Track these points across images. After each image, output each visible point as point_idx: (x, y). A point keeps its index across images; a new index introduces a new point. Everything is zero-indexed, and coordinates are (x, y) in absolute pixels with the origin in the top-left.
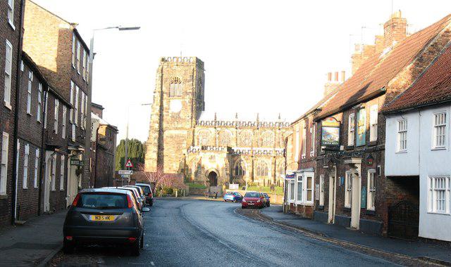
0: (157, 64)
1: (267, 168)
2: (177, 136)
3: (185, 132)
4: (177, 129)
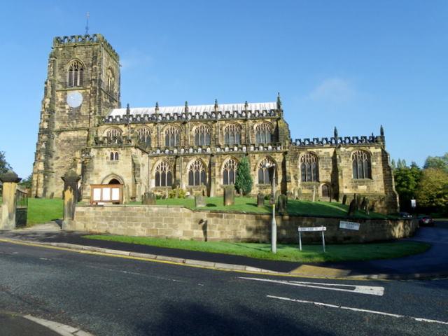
0: (48, 47)
4: (76, 129)
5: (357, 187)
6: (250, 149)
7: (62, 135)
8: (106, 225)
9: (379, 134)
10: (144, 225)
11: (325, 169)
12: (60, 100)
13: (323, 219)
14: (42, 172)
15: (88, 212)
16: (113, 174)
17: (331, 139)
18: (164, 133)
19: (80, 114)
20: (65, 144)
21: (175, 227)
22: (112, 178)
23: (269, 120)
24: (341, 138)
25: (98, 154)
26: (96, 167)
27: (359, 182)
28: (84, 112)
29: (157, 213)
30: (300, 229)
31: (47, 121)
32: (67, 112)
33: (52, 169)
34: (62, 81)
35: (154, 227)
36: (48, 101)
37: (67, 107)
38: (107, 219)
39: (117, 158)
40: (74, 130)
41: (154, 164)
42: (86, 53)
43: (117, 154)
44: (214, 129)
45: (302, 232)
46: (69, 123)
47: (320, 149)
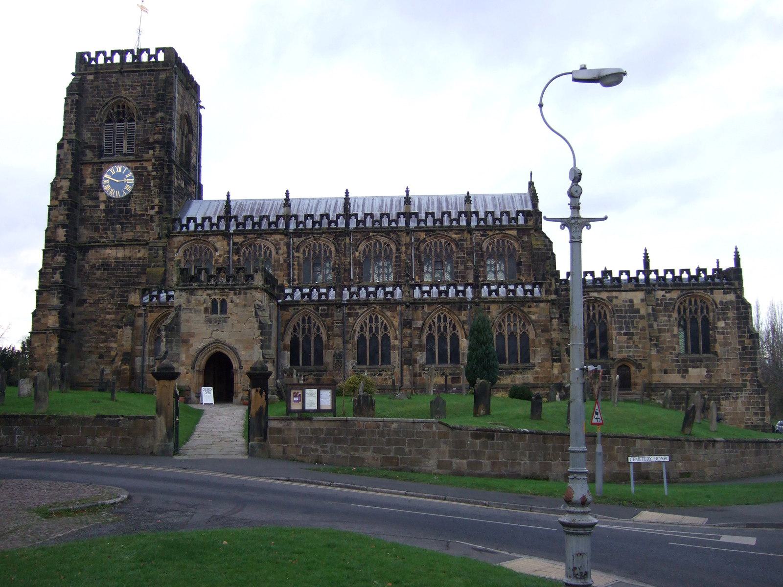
0: (66, 74)
1: (386, 338)
2: (122, 263)
3: (142, 253)
5: (686, 372)
6: (480, 293)
7: (92, 254)
8: (317, 450)
9: (732, 265)
10: (376, 451)
11: (626, 334)
12: (89, 181)
13: (648, 442)
14: (54, 331)
15: (289, 429)
16: (217, 341)
17: (638, 272)
18: (301, 256)
19: (128, 211)
20: (98, 273)
21: (425, 454)
23: (514, 233)
24: (656, 272)
25: (189, 301)
26: (184, 328)
27: (692, 361)
28: (135, 207)
29: (396, 432)
30: (631, 459)
31: (64, 226)
32: (102, 206)
33: (72, 324)
34: (94, 142)
35: (392, 455)
36: (65, 184)
37: (102, 197)
38: (318, 441)
39: (224, 310)
40: (116, 246)
41: (288, 321)
42: (143, 85)
43: (224, 302)
44: (403, 248)
45: (635, 464)
46: (105, 230)
47: (614, 294)
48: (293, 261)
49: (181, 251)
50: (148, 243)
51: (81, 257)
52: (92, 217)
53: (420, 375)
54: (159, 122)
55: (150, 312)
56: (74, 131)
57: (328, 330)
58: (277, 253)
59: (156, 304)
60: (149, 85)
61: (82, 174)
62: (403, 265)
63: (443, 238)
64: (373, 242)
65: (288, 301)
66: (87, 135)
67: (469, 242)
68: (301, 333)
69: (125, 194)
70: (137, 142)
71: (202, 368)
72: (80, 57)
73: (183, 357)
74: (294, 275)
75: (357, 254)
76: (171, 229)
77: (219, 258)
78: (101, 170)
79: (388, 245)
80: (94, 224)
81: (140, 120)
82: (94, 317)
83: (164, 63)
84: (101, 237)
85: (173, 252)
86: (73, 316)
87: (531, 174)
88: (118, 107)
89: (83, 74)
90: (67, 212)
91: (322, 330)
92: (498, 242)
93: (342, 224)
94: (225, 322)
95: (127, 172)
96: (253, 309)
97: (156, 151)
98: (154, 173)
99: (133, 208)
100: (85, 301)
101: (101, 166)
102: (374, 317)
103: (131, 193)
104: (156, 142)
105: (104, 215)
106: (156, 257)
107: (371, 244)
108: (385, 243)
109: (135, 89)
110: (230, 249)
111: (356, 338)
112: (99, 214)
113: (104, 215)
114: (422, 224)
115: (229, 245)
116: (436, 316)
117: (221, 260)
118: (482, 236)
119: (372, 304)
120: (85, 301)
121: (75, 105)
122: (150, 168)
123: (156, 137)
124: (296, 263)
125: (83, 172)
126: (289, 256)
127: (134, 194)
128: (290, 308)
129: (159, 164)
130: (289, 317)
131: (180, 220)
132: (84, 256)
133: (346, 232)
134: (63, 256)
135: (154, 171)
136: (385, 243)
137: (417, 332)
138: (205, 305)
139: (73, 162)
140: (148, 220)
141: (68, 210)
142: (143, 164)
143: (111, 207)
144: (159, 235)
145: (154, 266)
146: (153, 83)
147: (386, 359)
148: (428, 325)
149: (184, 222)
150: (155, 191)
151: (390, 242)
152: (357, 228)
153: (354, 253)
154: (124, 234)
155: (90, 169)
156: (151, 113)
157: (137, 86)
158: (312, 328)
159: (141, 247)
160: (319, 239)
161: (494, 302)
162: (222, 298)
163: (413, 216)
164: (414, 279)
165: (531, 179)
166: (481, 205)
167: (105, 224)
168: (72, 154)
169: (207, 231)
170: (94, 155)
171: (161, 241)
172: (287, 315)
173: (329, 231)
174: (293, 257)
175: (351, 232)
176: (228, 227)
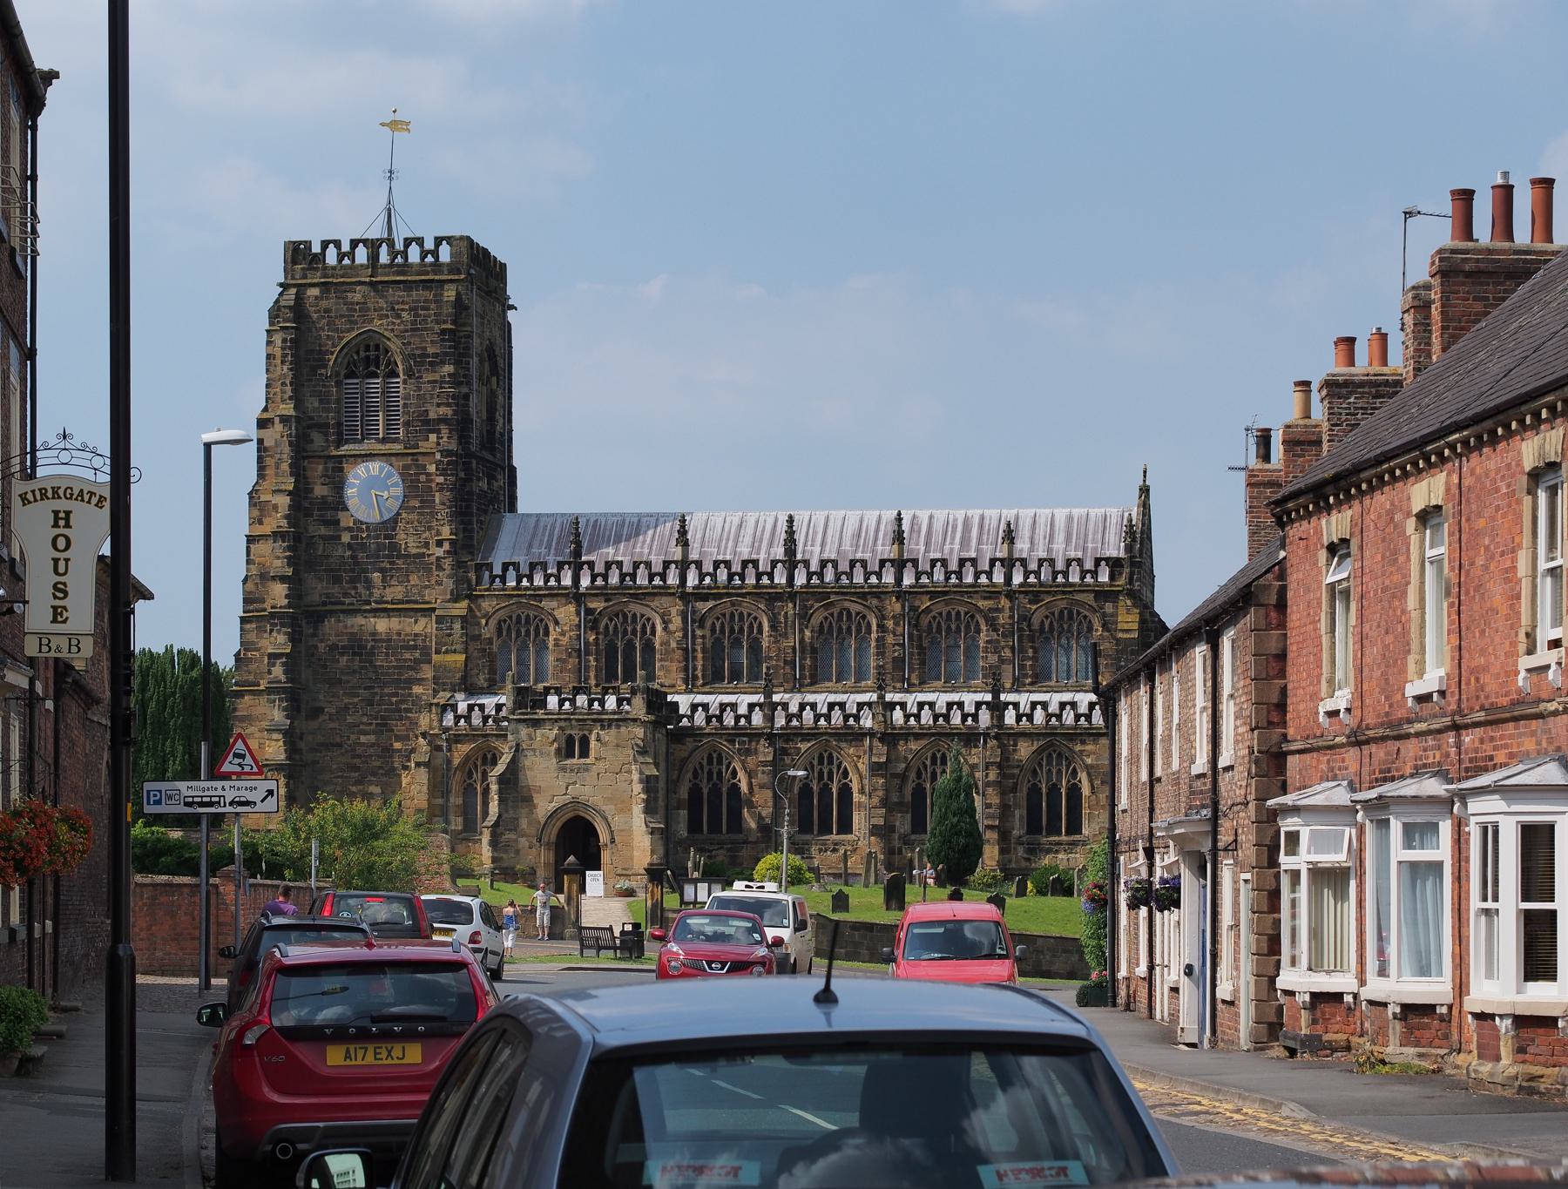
1: (845, 792)
6: (1002, 717)
7: (330, 625)
12: (320, 490)
16: (575, 802)
18: (708, 633)
19: (394, 547)
20: (344, 660)
22: (571, 815)
28: (408, 541)
31: (283, 579)
37: (346, 521)
39: (585, 753)
41: (684, 761)
43: (585, 742)
44: (890, 624)
46: (353, 581)
48: (694, 643)
49: (493, 622)
50: (434, 610)
51: (311, 631)
52: (327, 557)
53: (900, 852)
54: (446, 382)
55: (457, 742)
56: (290, 398)
57: (750, 777)
58: (665, 629)
59: (465, 729)
60: (423, 309)
61: (305, 478)
62: (889, 655)
63: (961, 605)
64: (836, 611)
65: (685, 728)
66: (313, 403)
67: (1007, 613)
68: (705, 781)
69: (387, 516)
70: (407, 417)
71: (553, 838)
72: (297, 253)
73: (524, 823)
74: (695, 668)
75: (807, 633)
76: (474, 582)
77: (561, 638)
78: (341, 470)
79: (864, 617)
80: (332, 570)
81: (410, 377)
82: (338, 739)
83: (453, 268)
84: (346, 595)
85: (479, 624)
86: (301, 739)
87: (1145, 472)
88: (367, 348)
89: (300, 285)
90: (288, 554)
91: (741, 775)
92: (1061, 612)
93: (780, 578)
94: (587, 770)
95: (389, 476)
96: (631, 752)
97: (442, 438)
98: (440, 479)
99: (403, 542)
100: (320, 710)
101: (341, 463)
102: (826, 755)
103: (398, 514)
104: (442, 420)
105: (348, 553)
106: (450, 635)
107: (832, 615)
108: (858, 614)
109: (399, 316)
110: (580, 621)
111: (796, 791)
112: (340, 552)
113: (348, 553)
114: (924, 580)
115: (578, 613)
116: (929, 755)
117: (565, 640)
118: (1030, 602)
119: (823, 734)
120: (320, 710)
121: (290, 348)
122: (432, 468)
123: (442, 410)
124: (699, 648)
125: (309, 473)
126: (685, 636)
127: (404, 515)
128: (688, 739)
129: (449, 463)
130: (686, 754)
131: (490, 567)
132: (316, 628)
133: (791, 594)
134: (285, 633)
135: (441, 475)
136: (858, 614)
137: (897, 781)
138: (556, 745)
139: (292, 458)
140: (432, 563)
141: (289, 548)
142: (417, 460)
143: (362, 538)
144: (452, 593)
145: (446, 652)
146: (433, 306)
147: (846, 827)
148: (915, 770)
149: (497, 570)
150: (443, 513)
151: (866, 612)
152: (808, 585)
153: (801, 631)
154: (388, 590)
155: (321, 467)
156: (431, 364)
157: (403, 310)
158: (724, 771)
159: (419, 614)
160: (740, 605)
161: (1024, 735)
162: (581, 733)
163: (909, 565)
164: (909, 679)
165: (1144, 481)
166: (1042, 533)
167: (353, 571)
168: (291, 444)
169: (540, 588)
170: (327, 441)
171: (457, 605)
172: (682, 751)
173: (758, 593)
174: (694, 636)
175: (797, 592)
176: (576, 580)
